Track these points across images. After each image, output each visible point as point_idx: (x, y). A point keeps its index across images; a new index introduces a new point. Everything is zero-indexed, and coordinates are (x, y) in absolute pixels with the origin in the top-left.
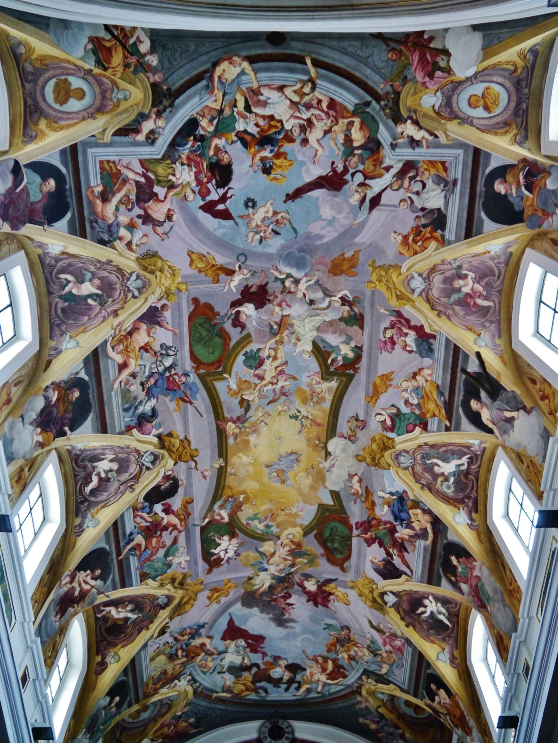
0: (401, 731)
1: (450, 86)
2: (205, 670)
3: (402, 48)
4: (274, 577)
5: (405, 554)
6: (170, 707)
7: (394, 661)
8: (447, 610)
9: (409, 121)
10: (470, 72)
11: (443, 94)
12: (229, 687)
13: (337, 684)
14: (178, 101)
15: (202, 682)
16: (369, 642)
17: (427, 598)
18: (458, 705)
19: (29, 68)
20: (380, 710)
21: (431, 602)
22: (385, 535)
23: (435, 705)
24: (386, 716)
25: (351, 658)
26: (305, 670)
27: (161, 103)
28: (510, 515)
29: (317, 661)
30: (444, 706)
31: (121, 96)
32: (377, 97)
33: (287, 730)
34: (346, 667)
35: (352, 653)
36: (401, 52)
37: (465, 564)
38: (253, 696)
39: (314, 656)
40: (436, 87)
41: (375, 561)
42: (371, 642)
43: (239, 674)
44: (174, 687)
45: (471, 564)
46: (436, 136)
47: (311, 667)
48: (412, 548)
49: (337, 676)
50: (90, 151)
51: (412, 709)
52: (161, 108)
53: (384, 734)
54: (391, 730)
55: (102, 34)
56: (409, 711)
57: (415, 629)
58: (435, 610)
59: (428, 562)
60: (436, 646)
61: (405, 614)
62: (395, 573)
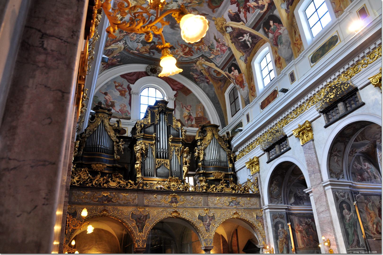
0: (208, 80)
2: (132, 40)
4: (179, 6)
5: (248, 13)
6: (112, 53)
7: (219, 55)
8: (252, 41)
12: (139, 49)
13: (186, 57)
15: (129, 45)
16: (210, 44)
17: (247, 34)
18: (242, 77)
20: (202, 71)
21: (247, 36)
22: (242, 2)
23: (230, 75)
24: (204, 74)
25: (198, 49)
26: (175, 49)
28: (306, 11)
29: (182, 46)
30: (235, 76)
33: (158, 71)
34: (194, 52)
35: (200, 47)
37: (276, 26)
38: (147, 55)
39: (181, 44)
41: (231, 12)
42: (211, 45)
43: (145, 45)
44: (117, 45)
45: (280, 27)
47: (178, 48)
48: (253, 12)
49: (188, 54)
51: (216, 73)
53: (199, 80)
54: (204, 79)
56: (214, 74)
57: (235, 45)
58: (247, 39)
59: (257, 20)
60: (241, 53)
61: (233, 38)
62: (238, 20)
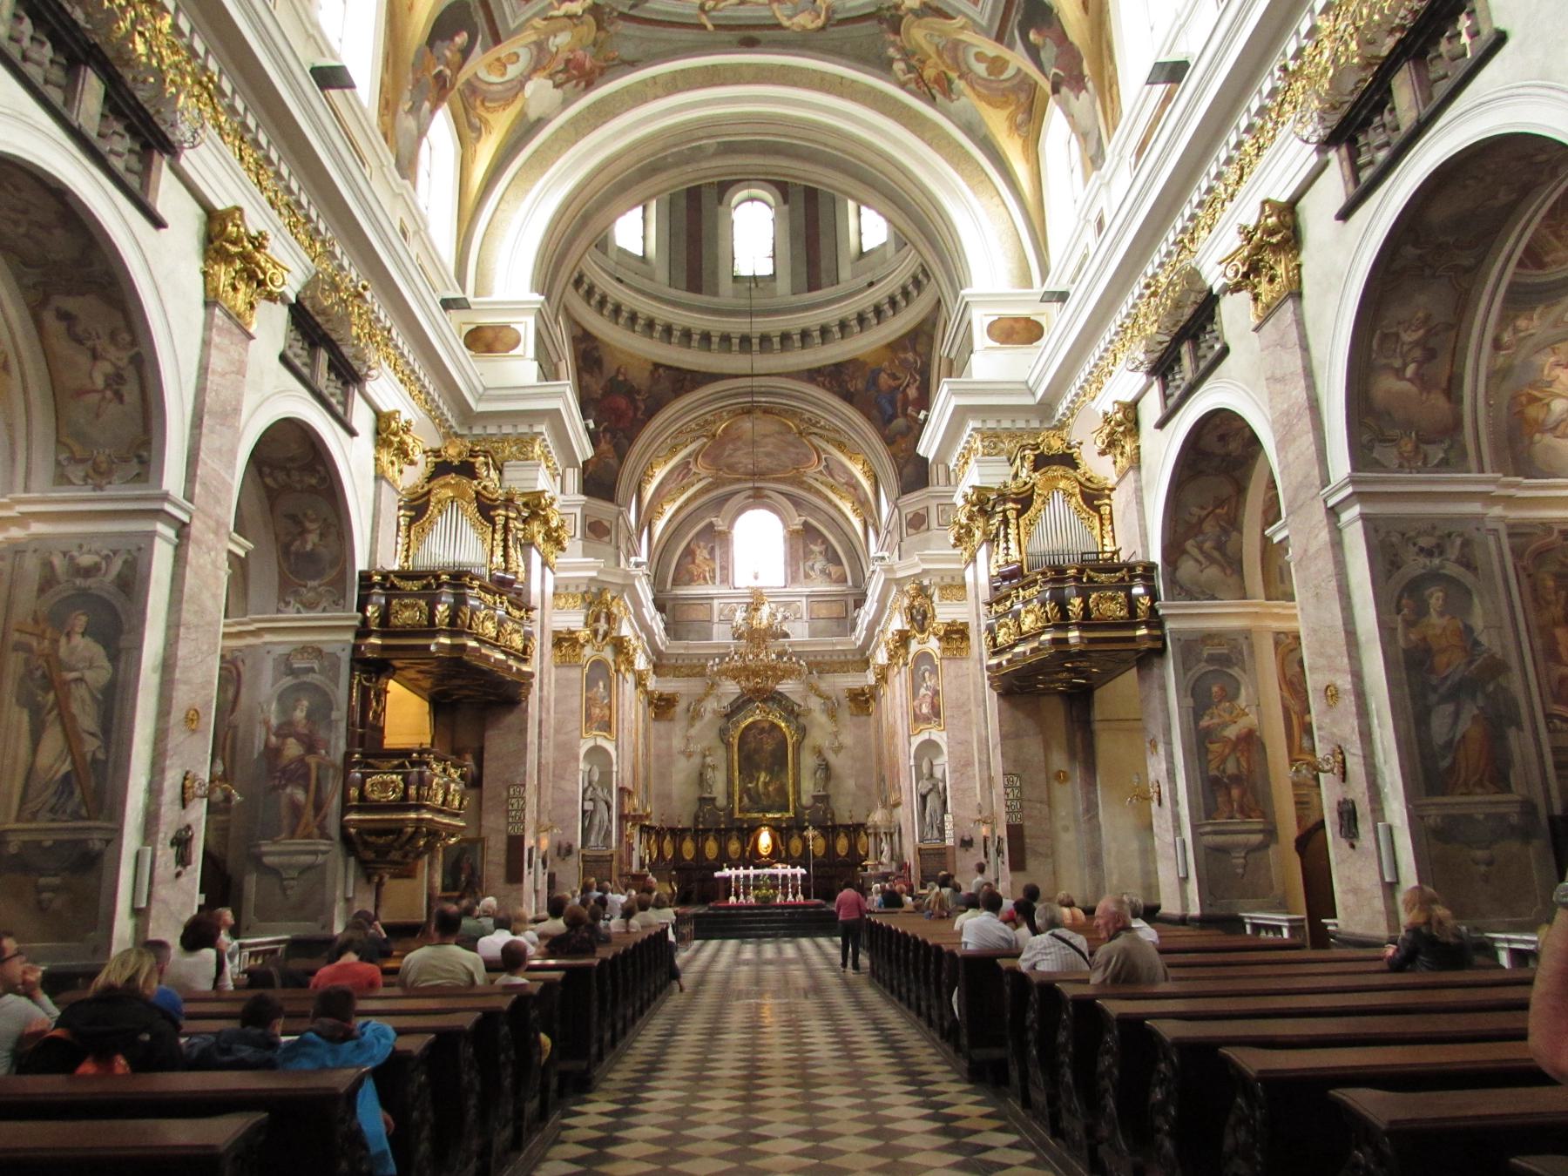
1: (545, 62)
3: (604, 64)
9: (580, 13)
10: (530, 87)
11: (550, 52)
14: (872, 9)
19: (1023, 97)
27: (892, 16)
31: (936, 39)
32: (623, 16)
36: (606, 61)
40: (560, 56)
46: (545, 19)
50: (984, 23)
52: (893, 12)
55: (939, 97)
